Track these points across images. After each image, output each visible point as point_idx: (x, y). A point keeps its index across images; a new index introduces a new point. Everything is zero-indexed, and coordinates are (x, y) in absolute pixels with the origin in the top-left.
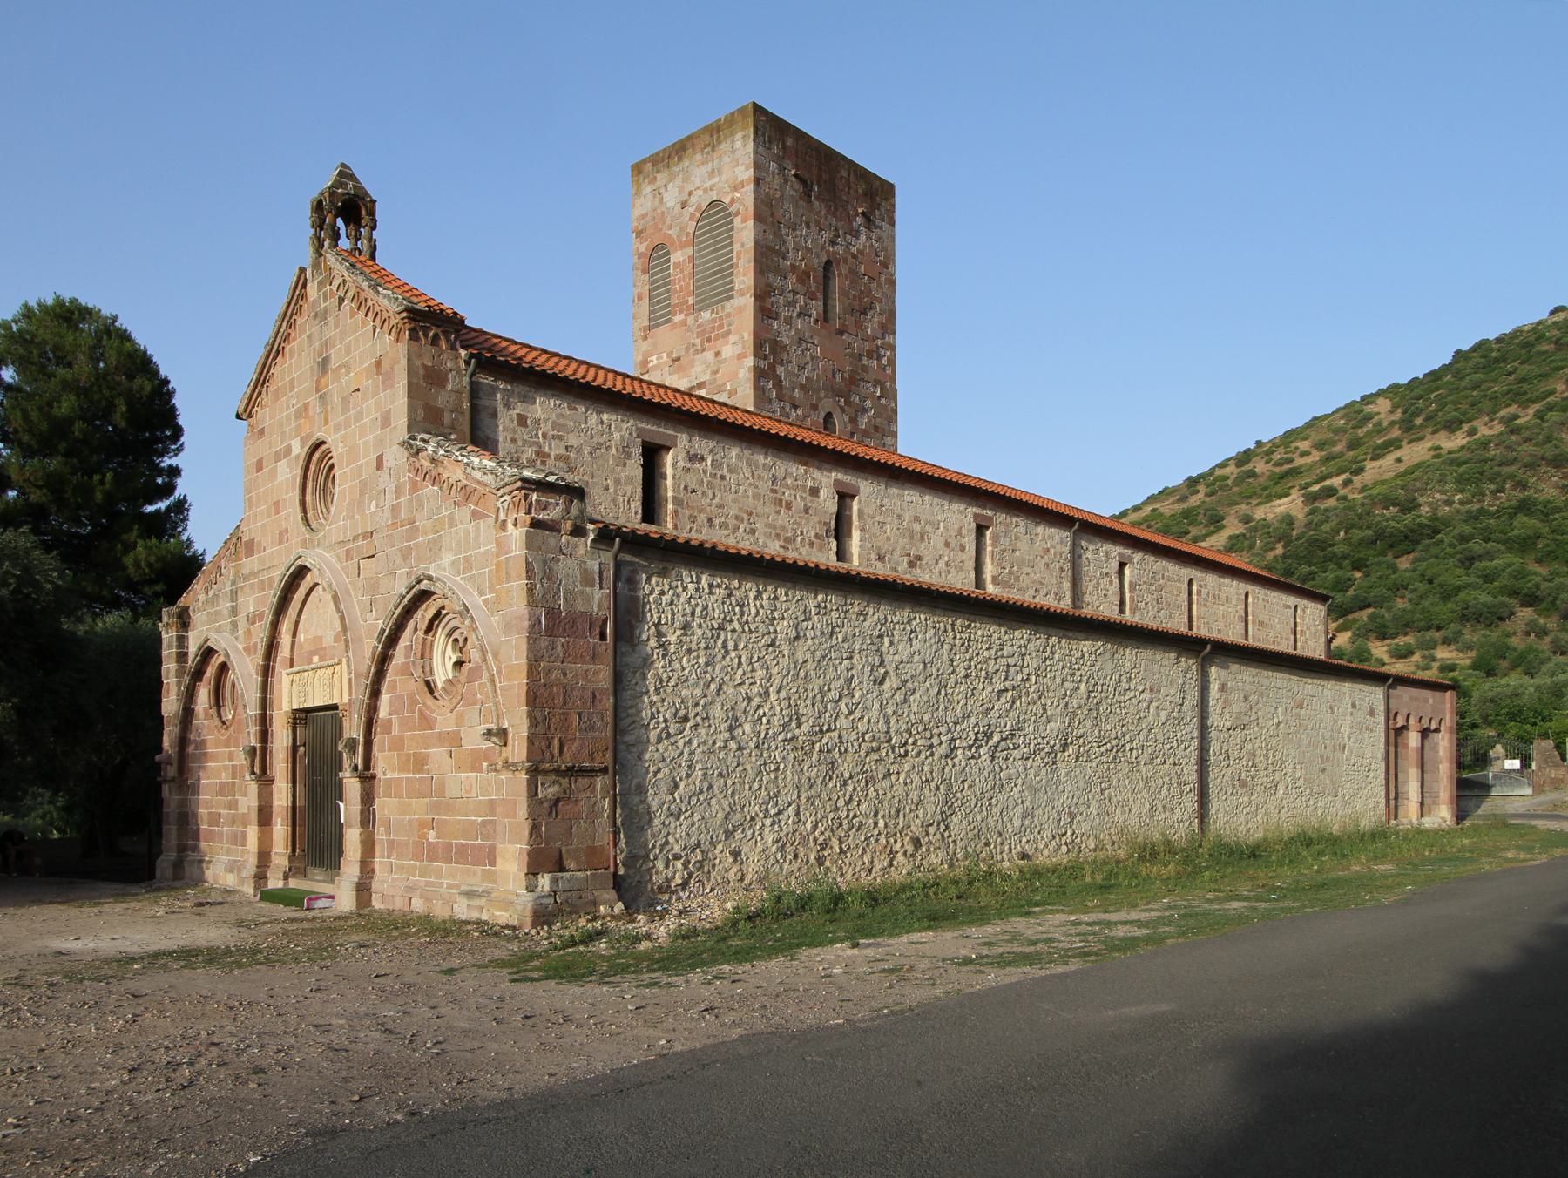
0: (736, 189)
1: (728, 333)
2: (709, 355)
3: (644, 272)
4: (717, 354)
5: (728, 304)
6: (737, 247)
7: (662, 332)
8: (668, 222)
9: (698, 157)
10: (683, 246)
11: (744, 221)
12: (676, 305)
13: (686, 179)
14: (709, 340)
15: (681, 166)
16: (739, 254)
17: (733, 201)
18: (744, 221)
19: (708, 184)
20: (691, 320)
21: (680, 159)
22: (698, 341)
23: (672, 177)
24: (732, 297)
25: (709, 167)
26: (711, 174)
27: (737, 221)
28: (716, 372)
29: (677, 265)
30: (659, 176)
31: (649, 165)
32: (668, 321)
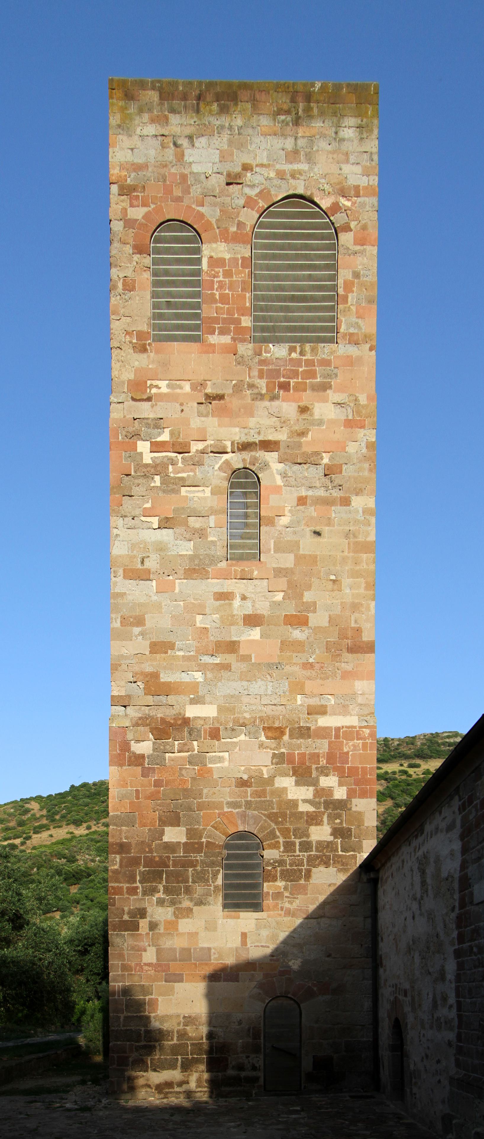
0: (343, 193)
1: (324, 387)
2: (288, 408)
3: (140, 249)
4: (304, 410)
5: (325, 350)
6: (344, 275)
7: (183, 355)
8: (196, 191)
9: (265, 121)
10: (226, 237)
11: (361, 241)
12: (216, 320)
13: (238, 142)
14: (285, 387)
15: (224, 120)
16: (348, 286)
17: (336, 208)
18: (361, 241)
19: (288, 167)
20: (246, 349)
21: (224, 110)
22: (262, 384)
23: (205, 131)
24: (331, 340)
25: (289, 144)
26: (293, 155)
27: (346, 239)
28: (303, 434)
29: (214, 262)
30: (174, 119)
31: (153, 96)
32: (196, 339)
